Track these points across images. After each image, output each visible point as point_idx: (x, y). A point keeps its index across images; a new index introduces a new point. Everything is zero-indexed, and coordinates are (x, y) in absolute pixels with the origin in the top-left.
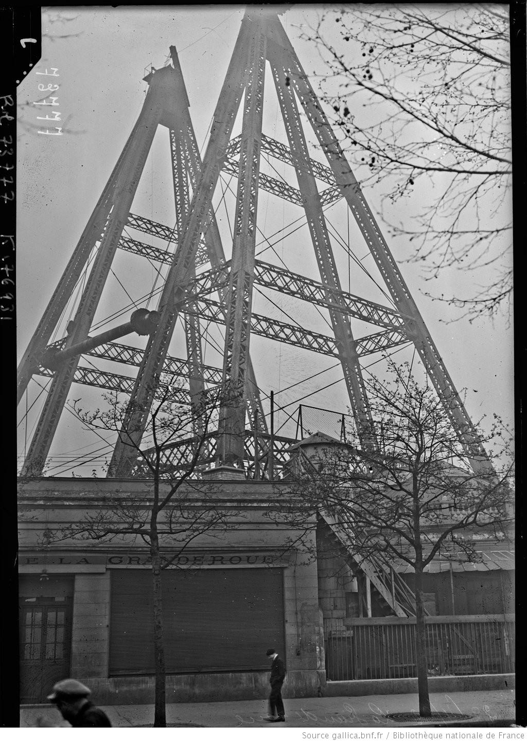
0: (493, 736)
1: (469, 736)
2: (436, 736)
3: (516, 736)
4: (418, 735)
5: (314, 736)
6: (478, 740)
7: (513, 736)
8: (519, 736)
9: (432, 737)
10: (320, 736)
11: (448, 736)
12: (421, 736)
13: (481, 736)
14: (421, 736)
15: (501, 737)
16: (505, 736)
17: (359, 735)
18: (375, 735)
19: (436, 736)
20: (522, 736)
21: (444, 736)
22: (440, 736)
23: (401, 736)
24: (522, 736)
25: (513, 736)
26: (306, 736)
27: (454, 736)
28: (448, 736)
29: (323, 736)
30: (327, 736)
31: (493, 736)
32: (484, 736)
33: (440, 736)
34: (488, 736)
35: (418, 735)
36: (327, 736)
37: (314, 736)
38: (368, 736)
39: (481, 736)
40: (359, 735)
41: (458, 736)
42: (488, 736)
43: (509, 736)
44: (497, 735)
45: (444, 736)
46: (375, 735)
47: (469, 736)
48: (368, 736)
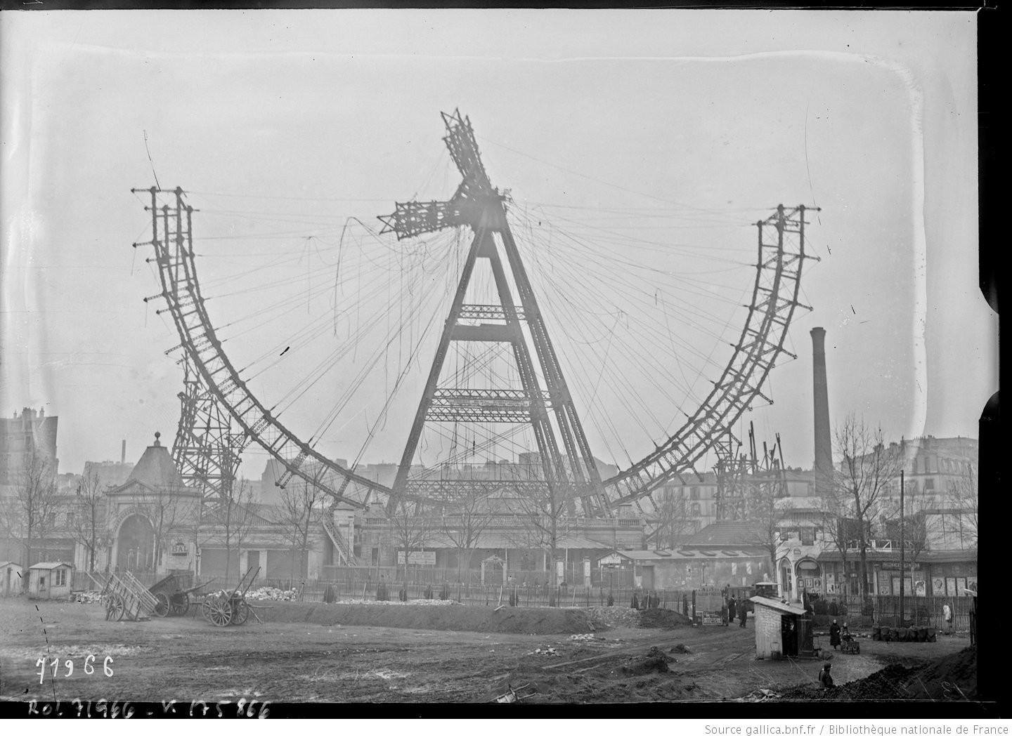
0: (966, 730)
1: (932, 730)
2: (887, 731)
3: (997, 731)
4: (863, 730)
5: (721, 731)
6: (944, 736)
7: (993, 730)
8: (1001, 730)
9: (882, 731)
10: (729, 730)
11: (904, 730)
12: (867, 730)
13: (949, 730)
14: (867, 730)
15: (977, 731)
16: (983, 731)
17: (783, 730)
18: (805, 729)
19: (887, 731)
20: (1006, 730)
21: (899, 730)
22: (894, 730)
23: (840, 730)
24: (1006, 730)
25: (993, 730)
26: (709, 731)
27: (913, 731)
28: (904, 730)
29: (734, 730)
30: (738, 730)
31: (966, 730)
32: (954, 731)
33: (894, 730)
34: (959, 731)
35: (863, 730)
36: (738, 730)
37: (721, 731)
38: (795, 730)
39: (949, 730)
40: (783, 730)
41: (918, 730)
42: (959, 731)
43: (988, 731)
44: (971, 730)
45: (899, 730)
46: (805, 729)
47: (932, 730)
48: (795, 730)
